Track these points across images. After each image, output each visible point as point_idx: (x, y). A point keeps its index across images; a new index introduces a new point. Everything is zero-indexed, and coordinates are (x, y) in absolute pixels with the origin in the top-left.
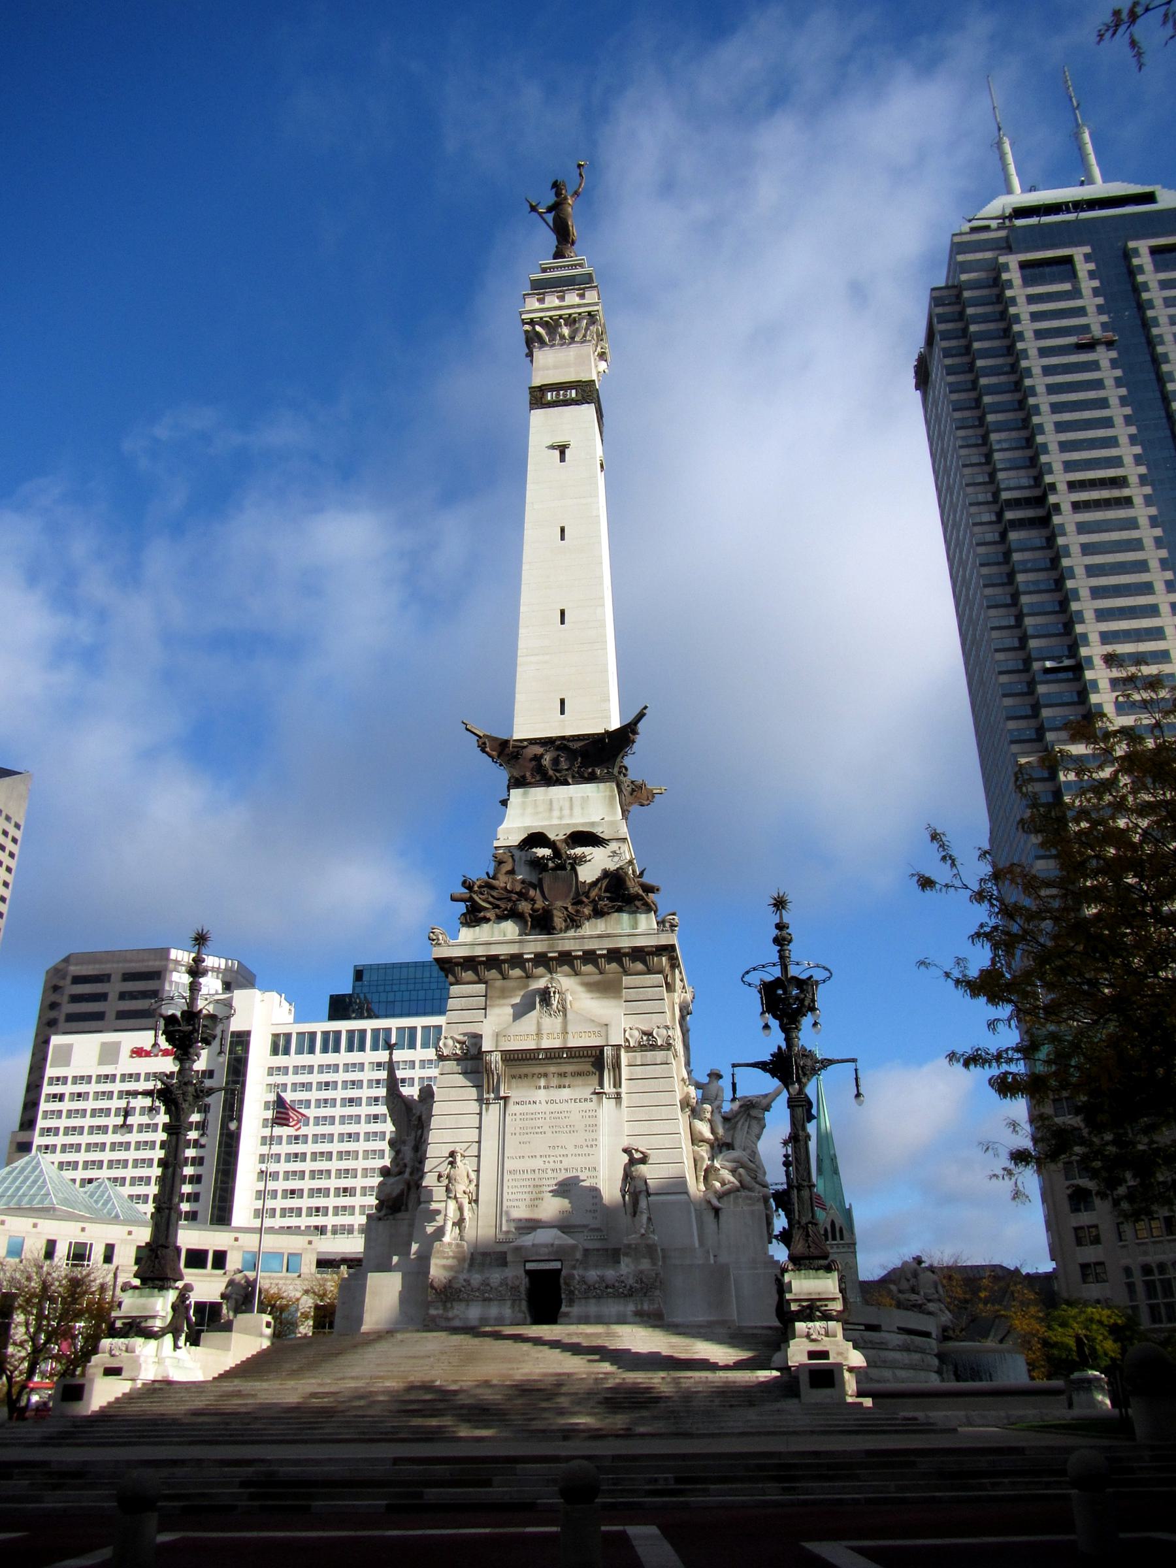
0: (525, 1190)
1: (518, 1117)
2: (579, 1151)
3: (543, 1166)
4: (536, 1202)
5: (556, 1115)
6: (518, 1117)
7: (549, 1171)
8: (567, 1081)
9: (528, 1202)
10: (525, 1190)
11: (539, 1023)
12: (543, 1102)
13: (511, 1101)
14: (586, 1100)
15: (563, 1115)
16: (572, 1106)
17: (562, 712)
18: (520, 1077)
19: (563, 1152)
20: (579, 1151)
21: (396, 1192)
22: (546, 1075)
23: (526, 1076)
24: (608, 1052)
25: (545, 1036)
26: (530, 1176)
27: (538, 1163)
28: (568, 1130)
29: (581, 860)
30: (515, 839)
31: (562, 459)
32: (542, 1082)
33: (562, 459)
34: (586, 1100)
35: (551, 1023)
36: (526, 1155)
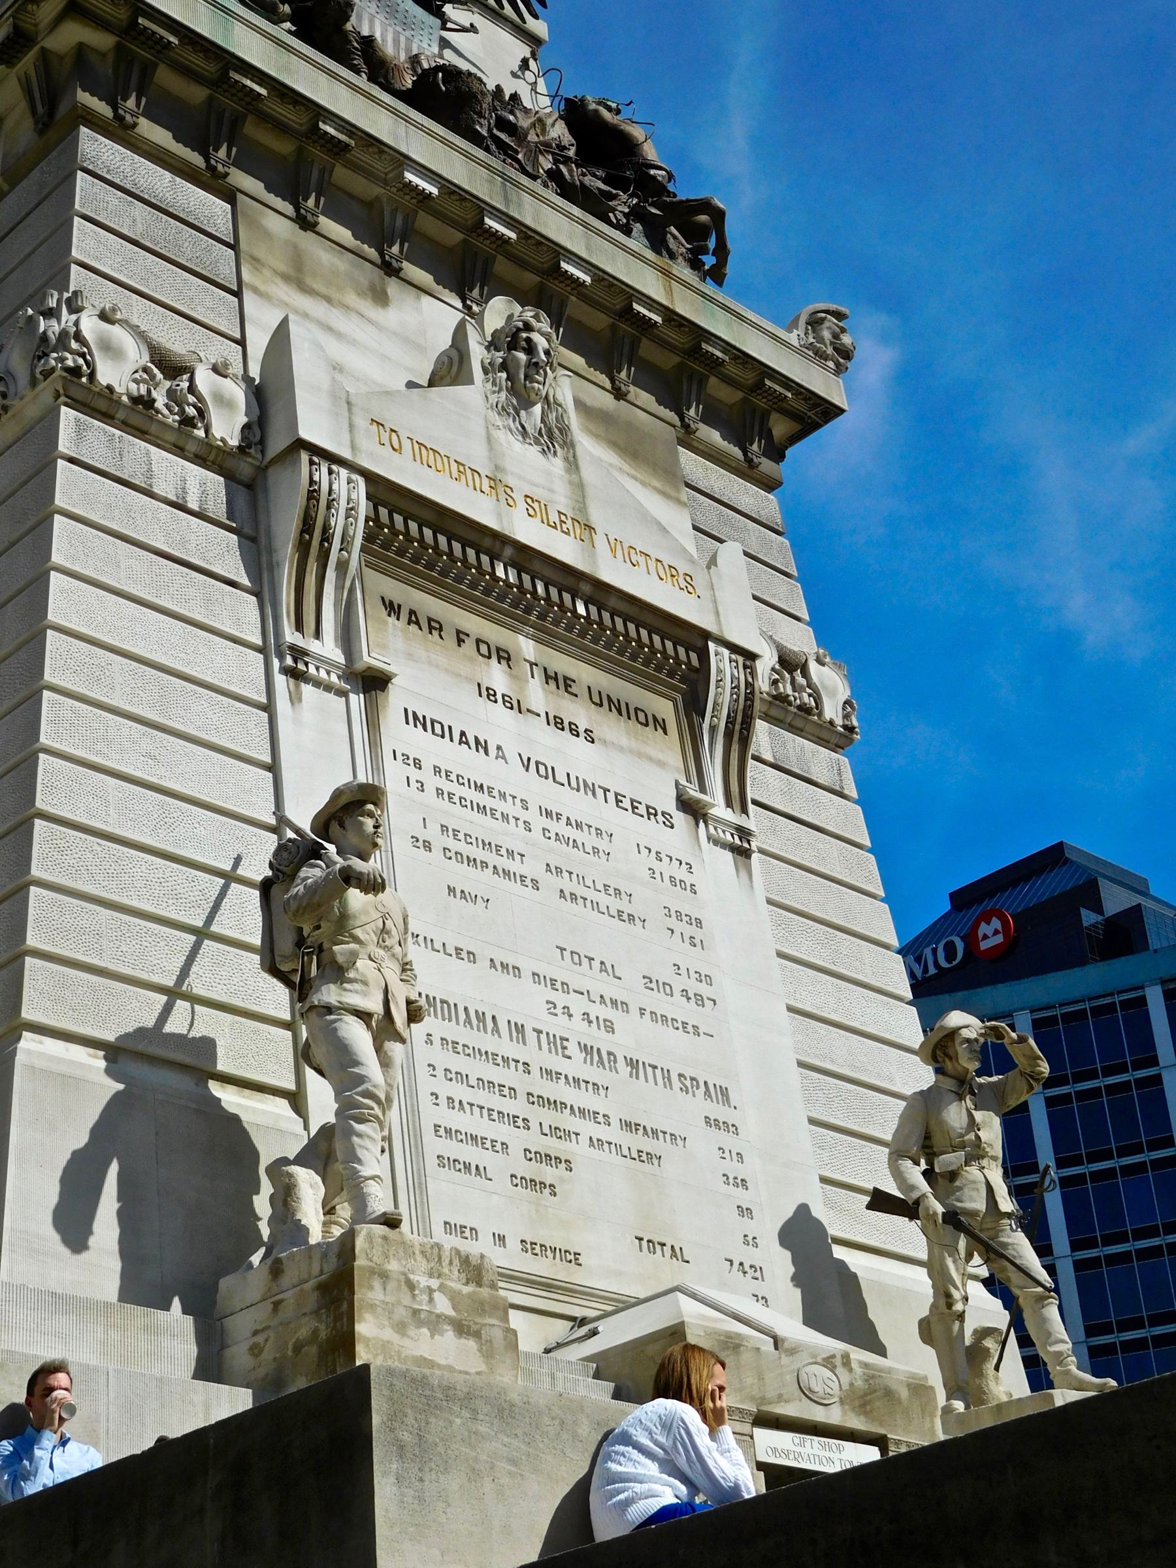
2: (657, 1002)
3: (557, 1025)
4: (549, 1174)
5: (560, 827)
6: (433, 782)
13: (396, 699)
15: (587, 838)
18: (413, 618)
19: (612, 990)
20: (657, 1002)
22: (504, 656)
23: (435, 626)
26: (506, 1046)
27: (523, 1002)
28: (615, 904)
36: (485, 953)
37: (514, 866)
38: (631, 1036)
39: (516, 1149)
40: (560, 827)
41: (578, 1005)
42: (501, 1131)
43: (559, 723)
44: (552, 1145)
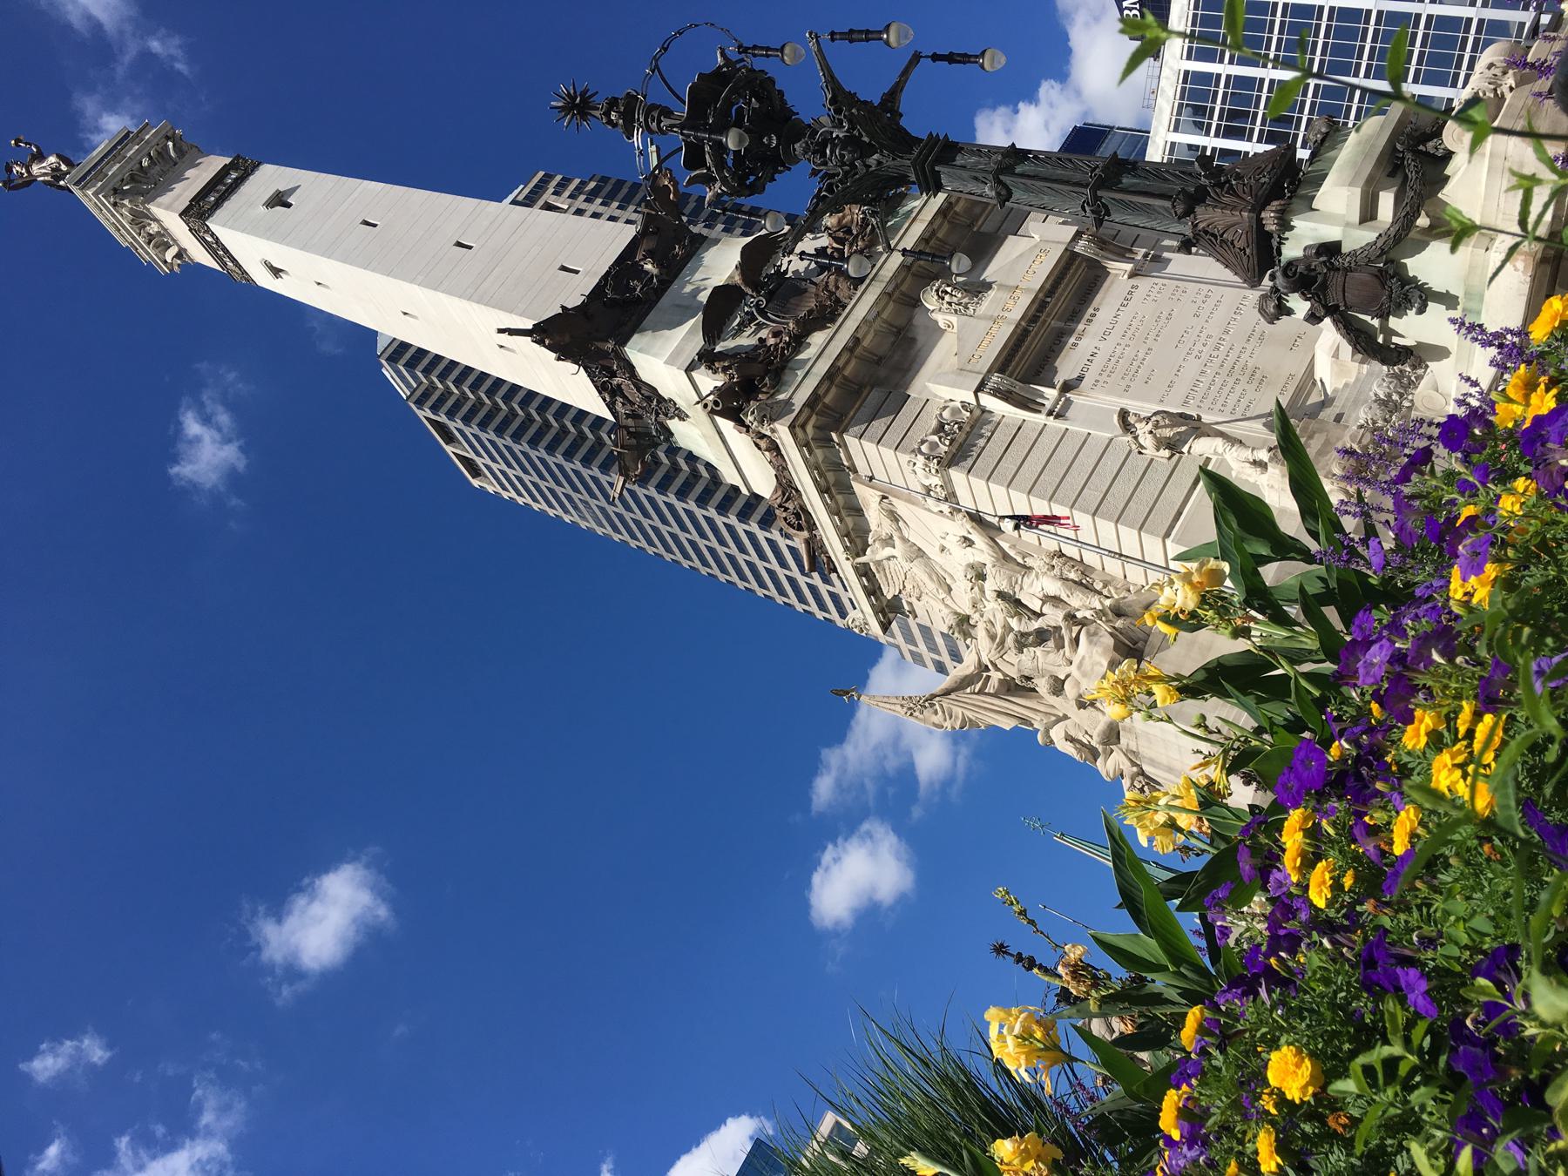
0: (1226, 390)
1: (1101, 379)
4: (1258, 376)
6: (1104, 377)
7: (1215, 353)
8: (1091, 311)
9: (1251, 388)
10: (1226, 390)
11: (979, 318)
12: (1101, 345)
14: (1130, 293)
16: (1125, 316)
17: (577, 272)
20: (1204, 314)
21: (1111, 641)
24: (1080, 248)
25: (1006, 314)
27: (1192, 368)
29: (780, 275)
30: (698, 342)
31: (289, 205)
32: (1072, 340)
33: (289, 205)
34: (1130, 293)
35: (990, 301)
37: (1141, 355)
38: (1214, 329)
39: (1247, 387)
40: (1129, 333)
41: (1199, 346)
42: (1239, 389)
43: (1090, 321)
44: (1248, 372)
